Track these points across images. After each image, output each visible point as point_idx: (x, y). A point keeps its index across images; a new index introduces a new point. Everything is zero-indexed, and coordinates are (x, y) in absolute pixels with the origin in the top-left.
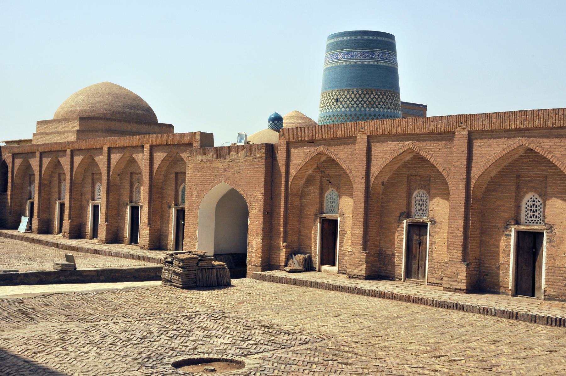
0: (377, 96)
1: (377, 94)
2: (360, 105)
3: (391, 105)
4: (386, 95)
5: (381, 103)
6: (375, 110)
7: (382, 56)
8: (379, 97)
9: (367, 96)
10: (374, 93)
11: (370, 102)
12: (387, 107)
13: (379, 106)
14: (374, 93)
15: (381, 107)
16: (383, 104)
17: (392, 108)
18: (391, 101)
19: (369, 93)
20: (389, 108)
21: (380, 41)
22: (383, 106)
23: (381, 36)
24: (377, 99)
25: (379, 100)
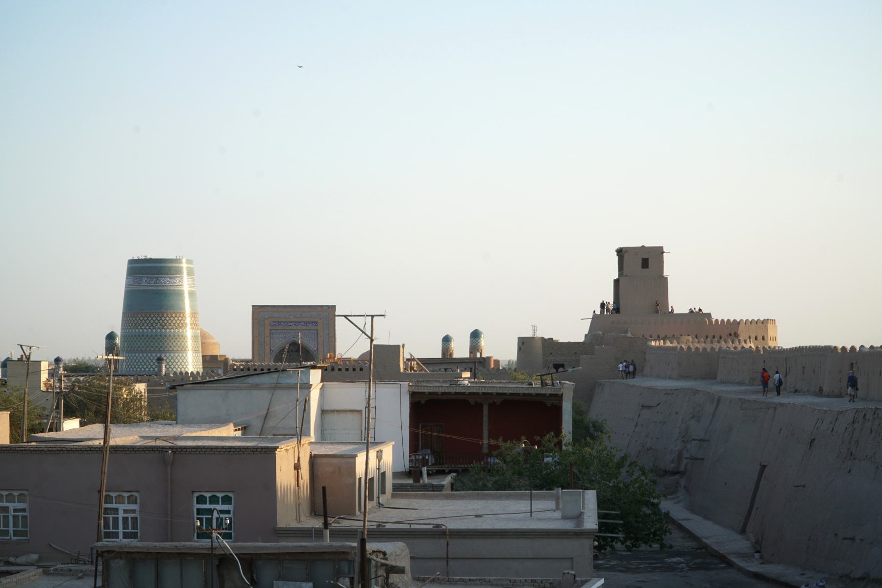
0: (141, 318)
1: (142, 316)
2: (129, 327)
3: (157, 325)
4: (150, 317)
5: (146, 324)
6: (139, 331)
7: (149, 281)
8: (143, 319)
9: (134, 319)
10: (139, 316)
11: (136, 324)
12: (152, 327)
13: (143, 327)
14: (139, 316)
15: (145, 328)
16: (148, 325)
17: (158, 328)
18: (157, 322)
19: (136, 316)
20: (154, 328)
21: (149, 267)
22: (147, 327)
23: (150, 263)
24: (141, 321)
25: (143, 322)
